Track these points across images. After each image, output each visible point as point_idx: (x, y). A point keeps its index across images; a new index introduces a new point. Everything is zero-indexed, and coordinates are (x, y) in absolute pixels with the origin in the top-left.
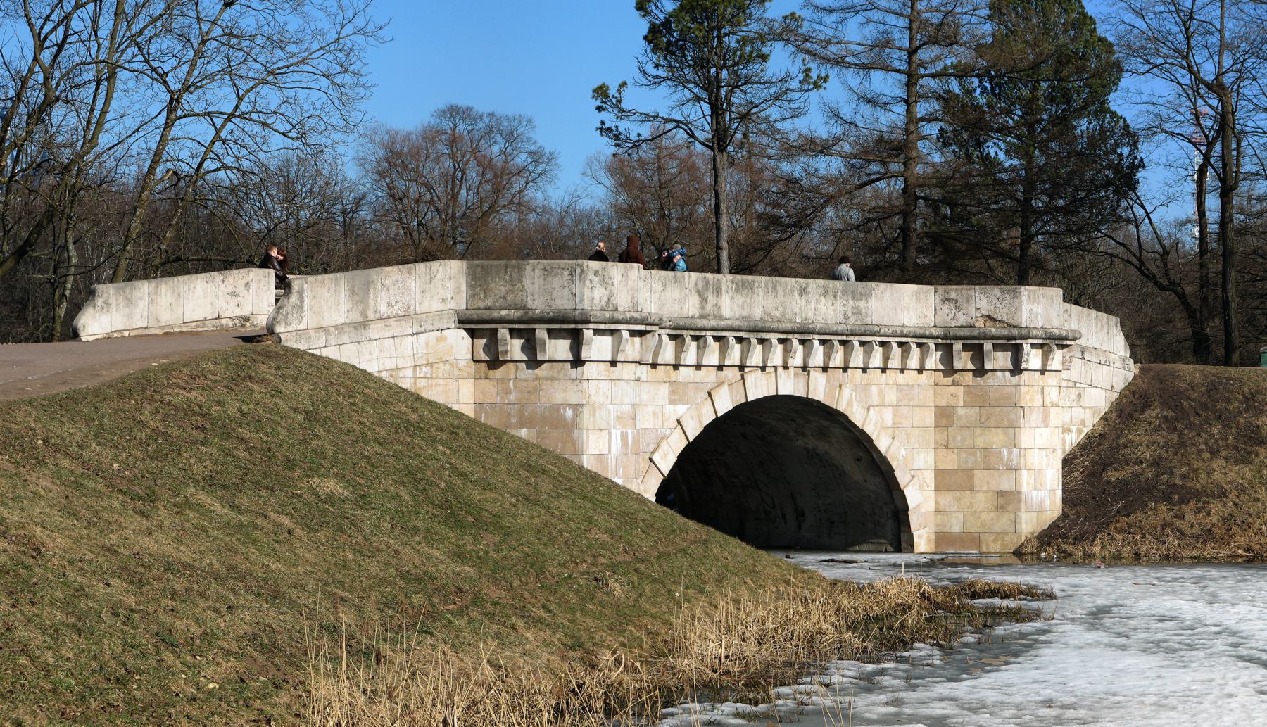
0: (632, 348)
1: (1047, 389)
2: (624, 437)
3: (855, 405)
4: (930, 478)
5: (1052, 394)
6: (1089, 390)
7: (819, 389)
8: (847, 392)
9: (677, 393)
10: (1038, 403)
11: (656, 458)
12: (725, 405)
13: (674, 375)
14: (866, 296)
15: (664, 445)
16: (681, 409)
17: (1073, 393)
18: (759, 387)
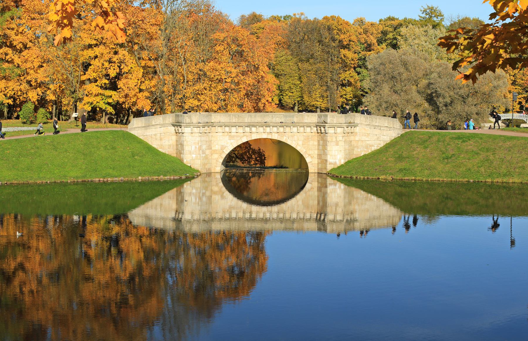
0: (196, 130)
1: (338, 137)
2: (196, 147)
3: (288, 140)
4: (316, 156)
5: (341, 138)
6: (382, 136)
7: (275, 137)
8: (285, 138)
9: (231, 137)
10: (334, 139)
11: (224, 151)
12: (245, 140)
13: (230, 134)
14: (293, 116)
15: (226, 148)
16: (232, 141)
17: (376, 137)
18: (254, 137)
